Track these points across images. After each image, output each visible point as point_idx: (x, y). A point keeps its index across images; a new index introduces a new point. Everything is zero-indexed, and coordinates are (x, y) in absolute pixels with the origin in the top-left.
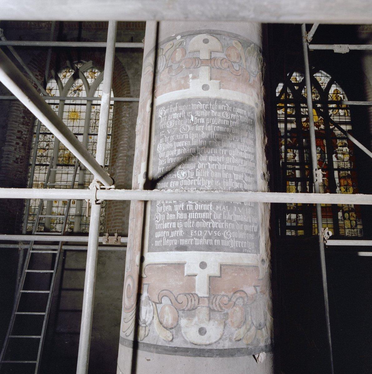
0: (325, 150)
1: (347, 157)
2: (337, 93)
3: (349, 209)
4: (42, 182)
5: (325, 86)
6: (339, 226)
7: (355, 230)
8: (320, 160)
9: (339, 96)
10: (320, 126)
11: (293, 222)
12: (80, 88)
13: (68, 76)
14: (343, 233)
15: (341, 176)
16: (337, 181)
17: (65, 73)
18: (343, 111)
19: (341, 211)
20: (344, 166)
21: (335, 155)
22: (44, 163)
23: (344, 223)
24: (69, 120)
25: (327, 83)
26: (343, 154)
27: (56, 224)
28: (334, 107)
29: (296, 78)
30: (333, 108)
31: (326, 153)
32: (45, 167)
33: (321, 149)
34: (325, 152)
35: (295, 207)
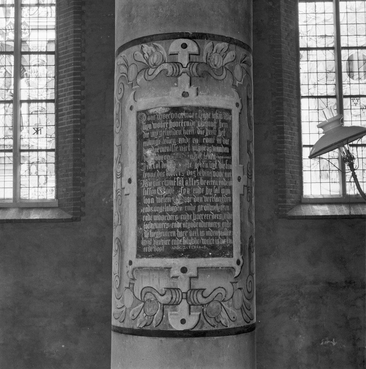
0: (11, 72)
1: (43, 83)
7: (45, 189)
14: (25, 193)
15: (31, 110)
33: (6, 72)
34: (11, 75)
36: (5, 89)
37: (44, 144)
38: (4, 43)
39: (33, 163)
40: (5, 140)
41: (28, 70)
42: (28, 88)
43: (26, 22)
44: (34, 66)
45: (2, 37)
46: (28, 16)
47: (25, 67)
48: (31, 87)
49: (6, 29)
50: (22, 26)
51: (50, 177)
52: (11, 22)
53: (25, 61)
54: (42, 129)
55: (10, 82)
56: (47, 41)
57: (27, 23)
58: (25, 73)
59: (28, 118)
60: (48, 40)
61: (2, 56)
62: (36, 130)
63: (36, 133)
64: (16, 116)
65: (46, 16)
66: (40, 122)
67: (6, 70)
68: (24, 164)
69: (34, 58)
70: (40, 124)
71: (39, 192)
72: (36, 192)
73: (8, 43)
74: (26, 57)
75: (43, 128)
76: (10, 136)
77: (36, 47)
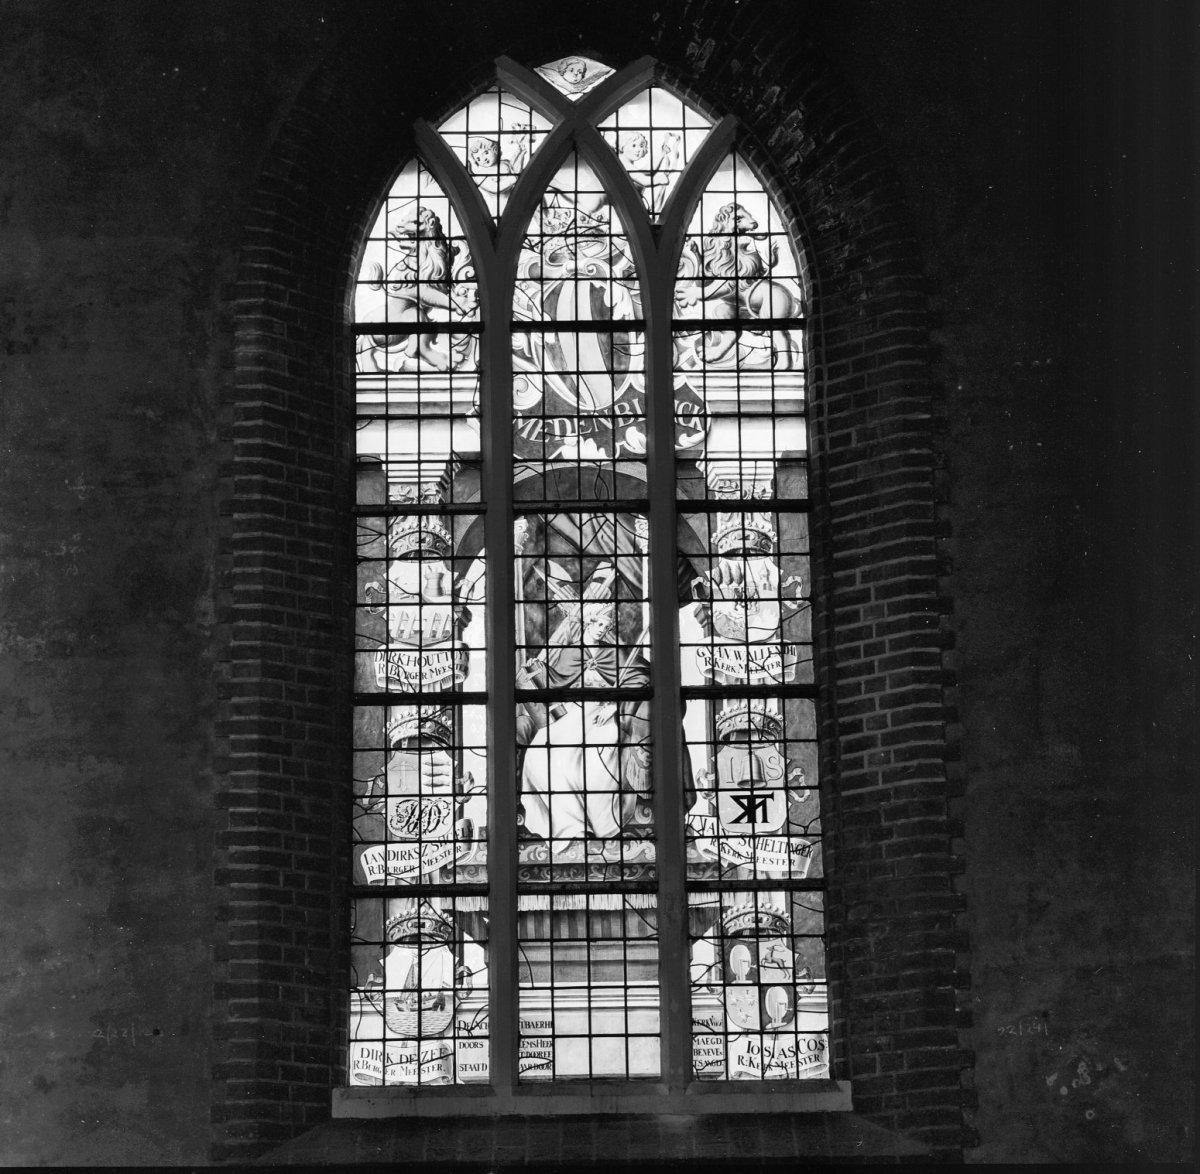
0: (640, 580)
1: (766, 618)
2: (738, 232)
3: (757, 921)
5: (669, 190)
6: (693, 1022)
7: (787, 1041)
8: (611, 639)
9: (745, 247)
10: (616, 434)
11: (435, 1007)
14: (711, 1058)
15: (725, 728)
16: (699, 757)
18: (762, 340)
19: (710, 932)
20: (748, 670)
21: (693, 607)
23: (725, 1005)
25: (681, 166)
26: (744, 599)
28: (710, 316)
29: (497, 145)
30: (706, 326)
31: (645, 595)
33: (620, 578)
35: (445, 923)
36: (618, 646)
37: (781, 862)
38: (608, 466)
39: (738, 935)
40: (625, 847)
41: (708, 573)
42: (708, 640)
43: (692, 388)
44: (731, 554)
45: (598, 448)
46: (699, 366)
47: (695, 561)
48: (719, 635)
49: (613, 417)
50: (676, 402)
51: (806, 991)
52: (631, 387)
53: (693, 536)
54: (769, 800)
55: (639, 618)
56: (774, 460)
57: (695, 390)
58: (694, 583)
59: (713, 758)
60: (779, 456)
61: (602, 520)
62: (746, 804)
63: (746, 819)
64: (667, 749)
65: (768, 366)
66: (759, 773)
67: (617, 570)
68: (703, 938)
69: (729, 524)
70: (761, 780)
71: (766, 1053)
72: (756, 1050)
73: (624, 468)
74: (696, 522)
75: (772, 796)
76: (643, 827)
77: (734, 485)
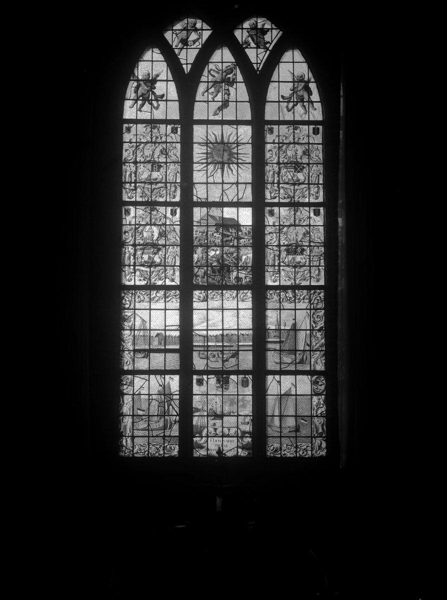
4: (159, 332)
12: (230, 76)
13: (194, 42)
17: (185, 32)
22: (160, 283)
24: (211, 167)
27: (207, 436)
32: (162, 293)
